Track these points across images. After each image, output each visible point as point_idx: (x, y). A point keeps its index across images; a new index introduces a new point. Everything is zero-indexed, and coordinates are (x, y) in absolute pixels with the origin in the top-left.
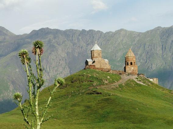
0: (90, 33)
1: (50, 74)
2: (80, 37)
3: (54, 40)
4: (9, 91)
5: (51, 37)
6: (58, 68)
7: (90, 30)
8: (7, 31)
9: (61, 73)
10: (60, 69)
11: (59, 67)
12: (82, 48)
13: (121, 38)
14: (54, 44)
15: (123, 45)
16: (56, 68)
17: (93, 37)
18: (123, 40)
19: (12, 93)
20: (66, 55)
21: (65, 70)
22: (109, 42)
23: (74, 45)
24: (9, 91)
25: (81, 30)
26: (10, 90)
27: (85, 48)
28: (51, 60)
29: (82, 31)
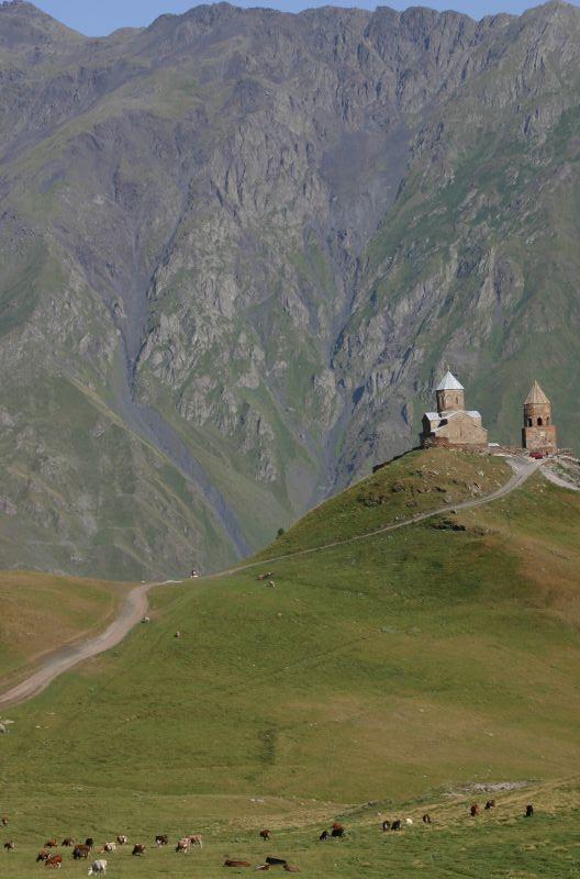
0: (412, 24)
1: (241, 213)
2: (369, 44)
3: (253, 61)
4: (66, 294)
5: (240, 44)
6: (276, 186)
7: (414, 12)
8: (47, 19)
9: (292, 209)
10: (288, 191)
11: (280, 181)
12: (378, 89)
13: (552, 44)
14: (254, 78)
15: (558, 74)
16: (267, 188)
17: (427, 41)
18: (558, 52)
19: (79, 303)
20: (308, 124)
21: (308, 195)
22: (497, 65)
23: (342, 80)
24: (66, 294)
25: (373, 9)
26: (72, 290)
27: (392, 90)
28: (246, 150)
29: (376, 14)
